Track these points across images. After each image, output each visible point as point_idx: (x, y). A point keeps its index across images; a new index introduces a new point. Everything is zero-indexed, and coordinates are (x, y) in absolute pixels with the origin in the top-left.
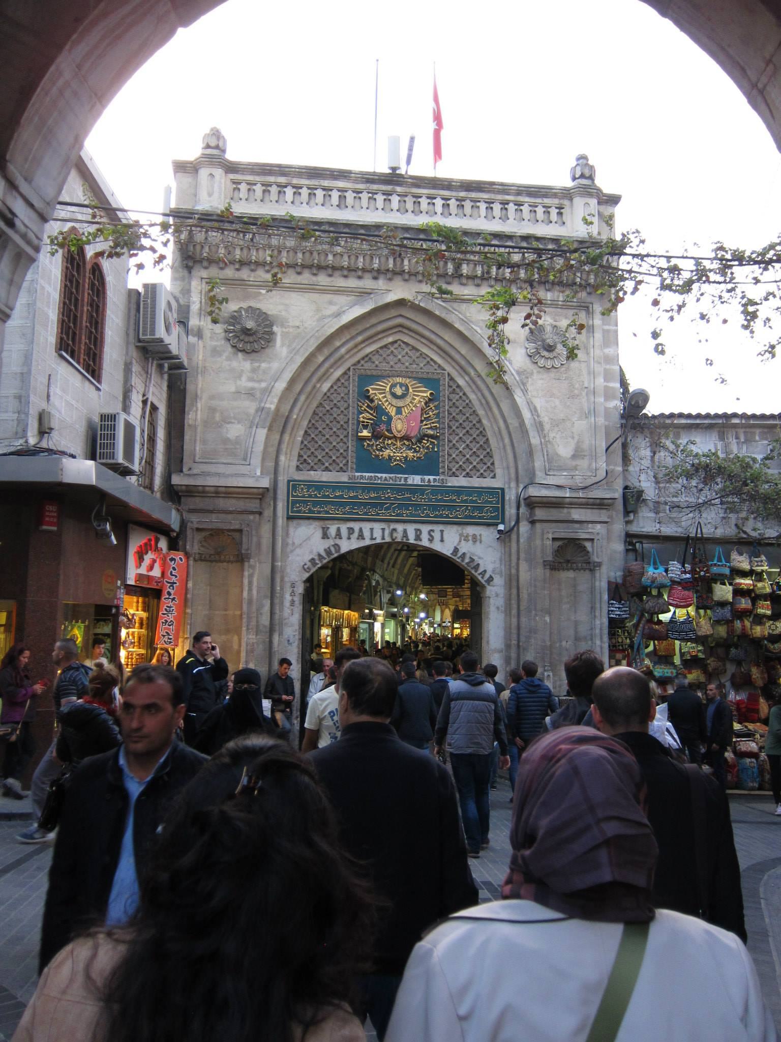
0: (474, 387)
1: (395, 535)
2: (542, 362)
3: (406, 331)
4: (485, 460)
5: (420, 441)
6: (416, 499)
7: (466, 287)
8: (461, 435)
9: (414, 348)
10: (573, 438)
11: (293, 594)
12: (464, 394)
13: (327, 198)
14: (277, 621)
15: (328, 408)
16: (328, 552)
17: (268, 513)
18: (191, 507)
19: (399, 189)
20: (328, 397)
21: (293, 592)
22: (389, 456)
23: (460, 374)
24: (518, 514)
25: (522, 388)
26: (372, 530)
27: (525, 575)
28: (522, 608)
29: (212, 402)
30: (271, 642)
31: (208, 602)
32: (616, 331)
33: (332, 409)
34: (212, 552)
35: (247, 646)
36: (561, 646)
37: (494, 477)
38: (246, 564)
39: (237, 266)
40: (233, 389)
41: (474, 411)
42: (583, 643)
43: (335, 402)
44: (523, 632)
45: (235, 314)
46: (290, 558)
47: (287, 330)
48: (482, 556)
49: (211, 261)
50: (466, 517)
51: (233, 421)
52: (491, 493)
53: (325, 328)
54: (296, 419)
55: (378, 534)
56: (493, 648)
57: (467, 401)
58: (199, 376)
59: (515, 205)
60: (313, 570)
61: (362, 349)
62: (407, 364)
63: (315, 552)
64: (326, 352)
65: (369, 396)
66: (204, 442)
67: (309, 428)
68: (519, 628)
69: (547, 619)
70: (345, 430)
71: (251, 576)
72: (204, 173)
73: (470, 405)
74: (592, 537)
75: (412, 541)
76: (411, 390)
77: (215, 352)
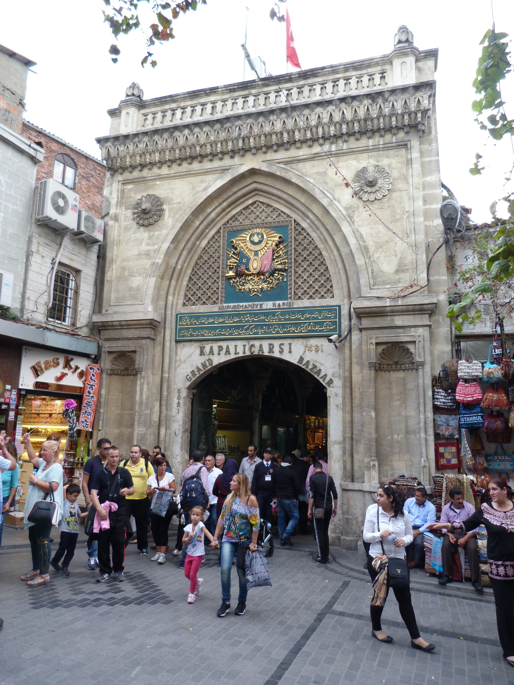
0: (314, 227)
1: (253, 349)
2: (365, 197)
3: (261, 193)
4: (325, 284)
5: (272, 274)
7: (301, 150)
8: (305, 266)
9: (269, 205)
10: (396, 255)
11: (179, 398)
12: (308, 234)
13: (204, 110)
14: (163, 418)
15: (206, 259)
16: (204, 365)
17: (159, 338)
18: (106, 337)
19: (253, 91)
20: (206, 251)
21: (179, 396)
22: (249, 288)
23: (303, 219)
24: (350, 325)
25: (349, 220)
26: (236, 346)
27: (356, 378)
28: (354, 405)
29: (124, 263)
30: (159, 433)
31: (120, 405)
32: (438, 161)
33: (209, 259)
34: (123, 368)
36: (392, 438)
38: (139, 375)
39: (139, 168)
40: (136, 252)
41: (316, 246)
42: (413, 436)
43: (211, 253)
44: (356, 427)
45: (139, 201)
46: (178, 371)
48: (323, 362)
49: (124, 169)
50: (309, 331)
52: (330, 310)
54: (181, 270)
55: (240, 350)
56: (333, 440)
57: (310, 239)
58: (115, 247)
59: (344, 80)
60: (193, 379)
61: (229, 212)
62: (263, 218)
63: (195, 366)
64: (201, 218)
65: (234, 246)
66: (117, 291)
67: (193, 275)
68: (352, 422)
69: (373, 414)
70: (218, 273)
71: (142, 385)
72: (124, 113)
73: (313, 242)
74: (413, 340)
75: (266, 353)
76: (265, 237)
77: (127, 229)
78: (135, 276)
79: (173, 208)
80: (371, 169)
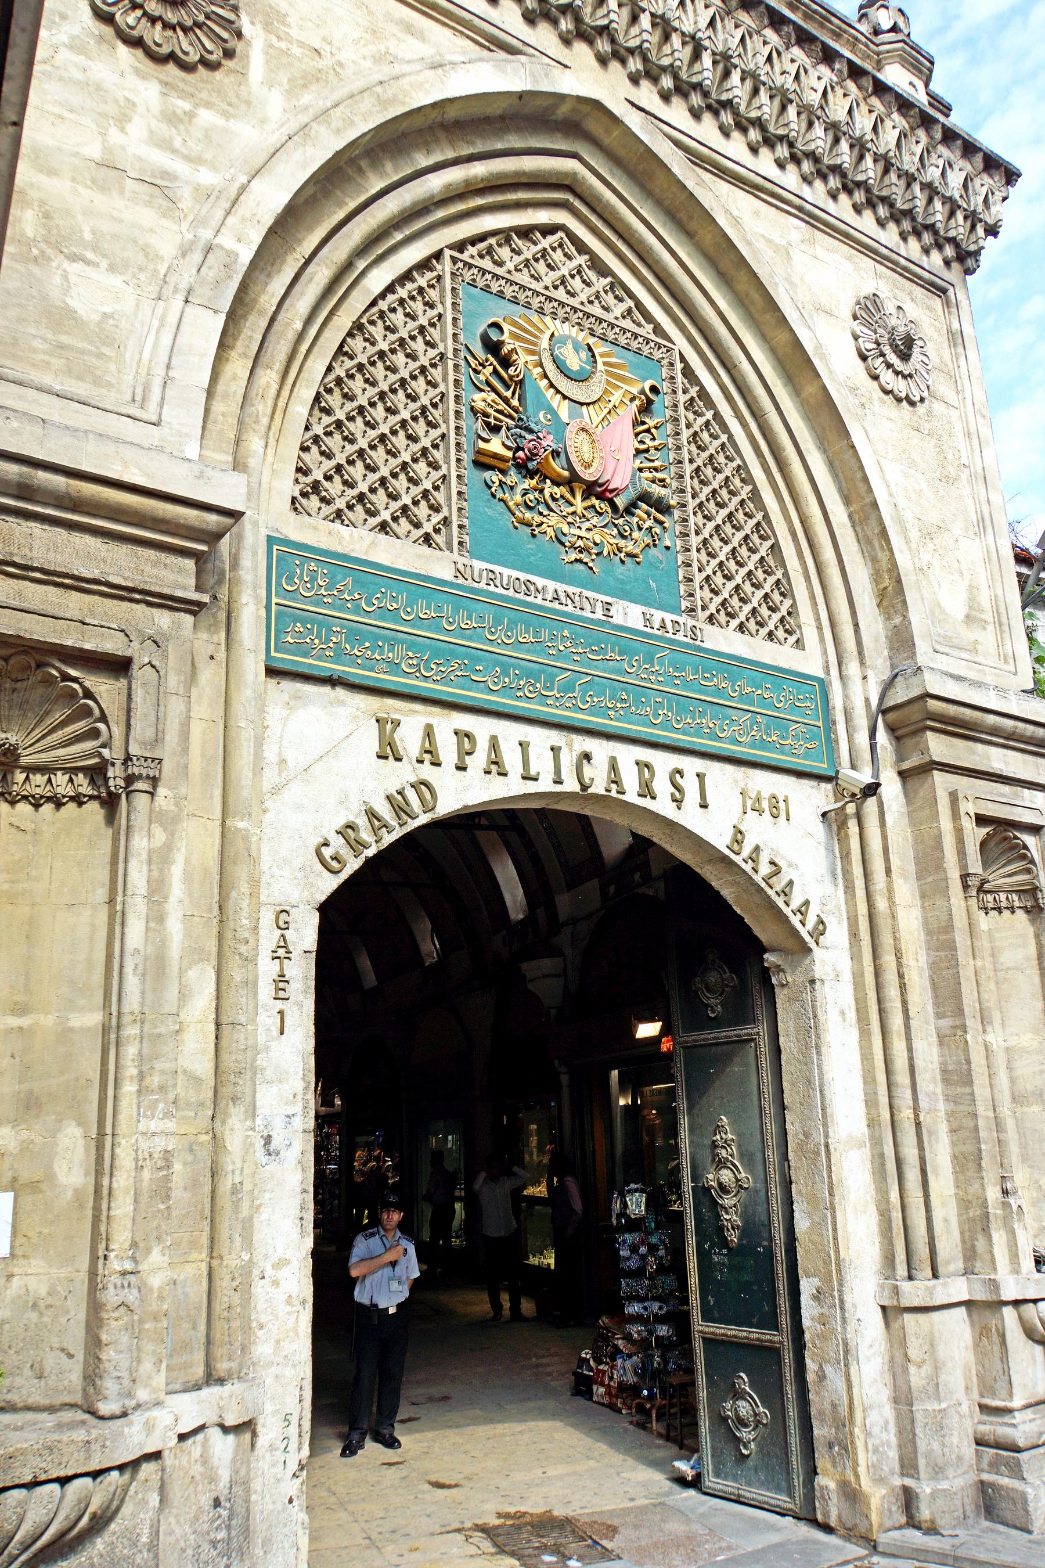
1: (588, 771)
2: (887, 377)
3: (584, 210)
6: (635, 671)
11: (282, 952)
21: (284, 944)
35: (139, 1169)
37: (799, 644)
40: (95, 151)
47: (283, 45)
51: (90, 255)
53: (404, 82)
55: (542, 763)
60: (353, 865)
71: (161, 858)
73: (730, 451)
75: (631, 796)
76: (600, 366)
78: (88, 262)
79: (286, 53)
80: (890, 307)
